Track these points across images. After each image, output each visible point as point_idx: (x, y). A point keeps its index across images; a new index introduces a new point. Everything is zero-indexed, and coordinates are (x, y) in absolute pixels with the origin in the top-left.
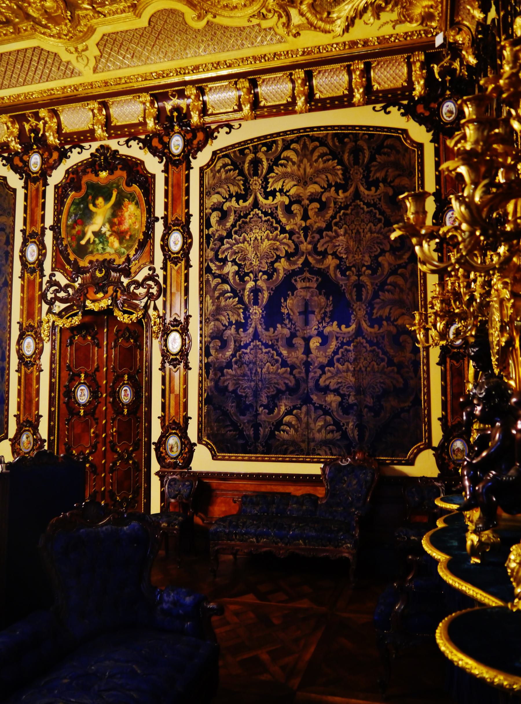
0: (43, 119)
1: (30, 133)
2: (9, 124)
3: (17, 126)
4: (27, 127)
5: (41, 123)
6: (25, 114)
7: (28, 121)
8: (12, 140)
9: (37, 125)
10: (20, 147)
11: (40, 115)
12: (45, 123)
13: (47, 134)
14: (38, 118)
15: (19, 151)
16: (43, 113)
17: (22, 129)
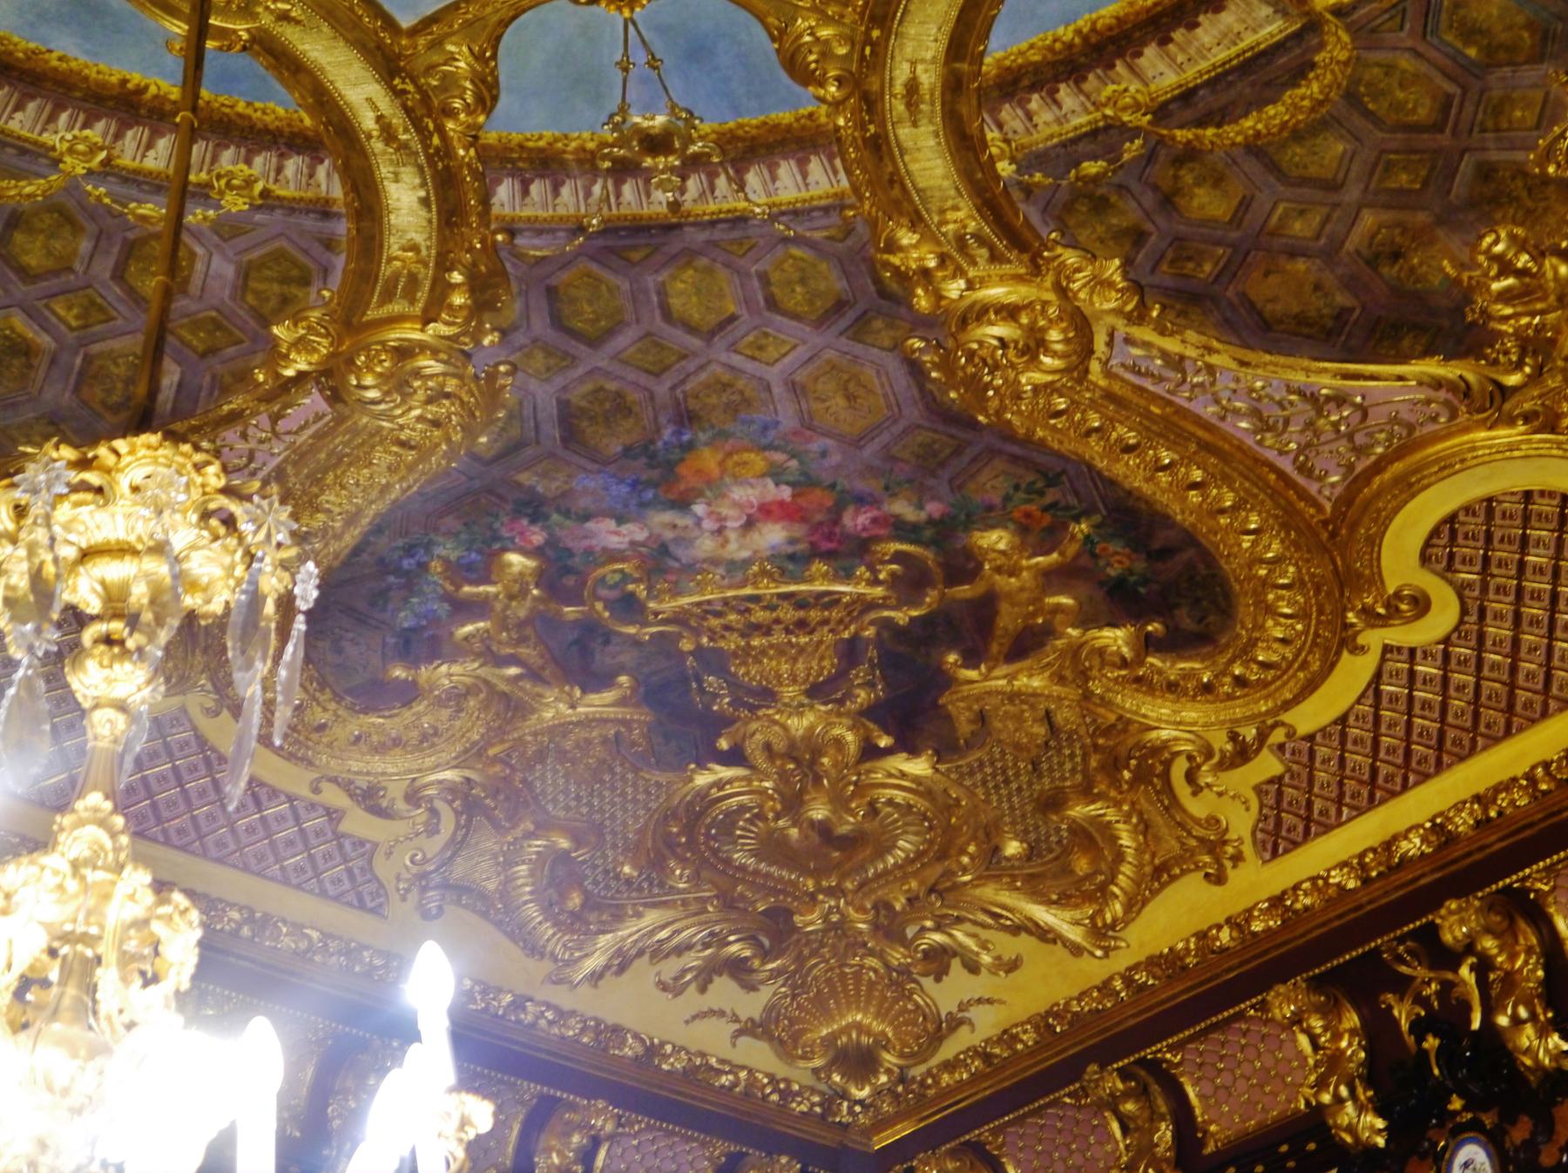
0: (1470, 948)
1: (1420, 1039)
2: (1317, 1024)
3: (1352, 1019)
4: (1403, 1014)
5: (1465, 972)
6: (1377, 951)
7: (1402, 985)
8: (1339, 1100)
9: (1447, 987)
10: (1380, 1124)
11: (1447, 938)
12: (1484, 966)
13: (1503, 1021)
14: (1446, 958)
15: (1380, 1141)
16: (1455, 925)
17: (1377, 1030)
